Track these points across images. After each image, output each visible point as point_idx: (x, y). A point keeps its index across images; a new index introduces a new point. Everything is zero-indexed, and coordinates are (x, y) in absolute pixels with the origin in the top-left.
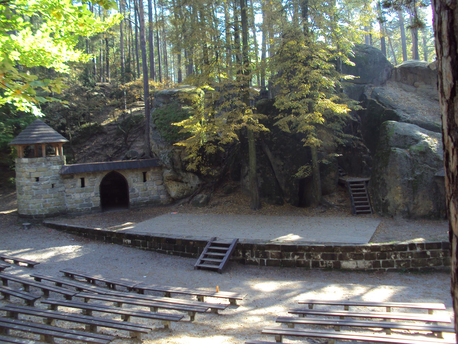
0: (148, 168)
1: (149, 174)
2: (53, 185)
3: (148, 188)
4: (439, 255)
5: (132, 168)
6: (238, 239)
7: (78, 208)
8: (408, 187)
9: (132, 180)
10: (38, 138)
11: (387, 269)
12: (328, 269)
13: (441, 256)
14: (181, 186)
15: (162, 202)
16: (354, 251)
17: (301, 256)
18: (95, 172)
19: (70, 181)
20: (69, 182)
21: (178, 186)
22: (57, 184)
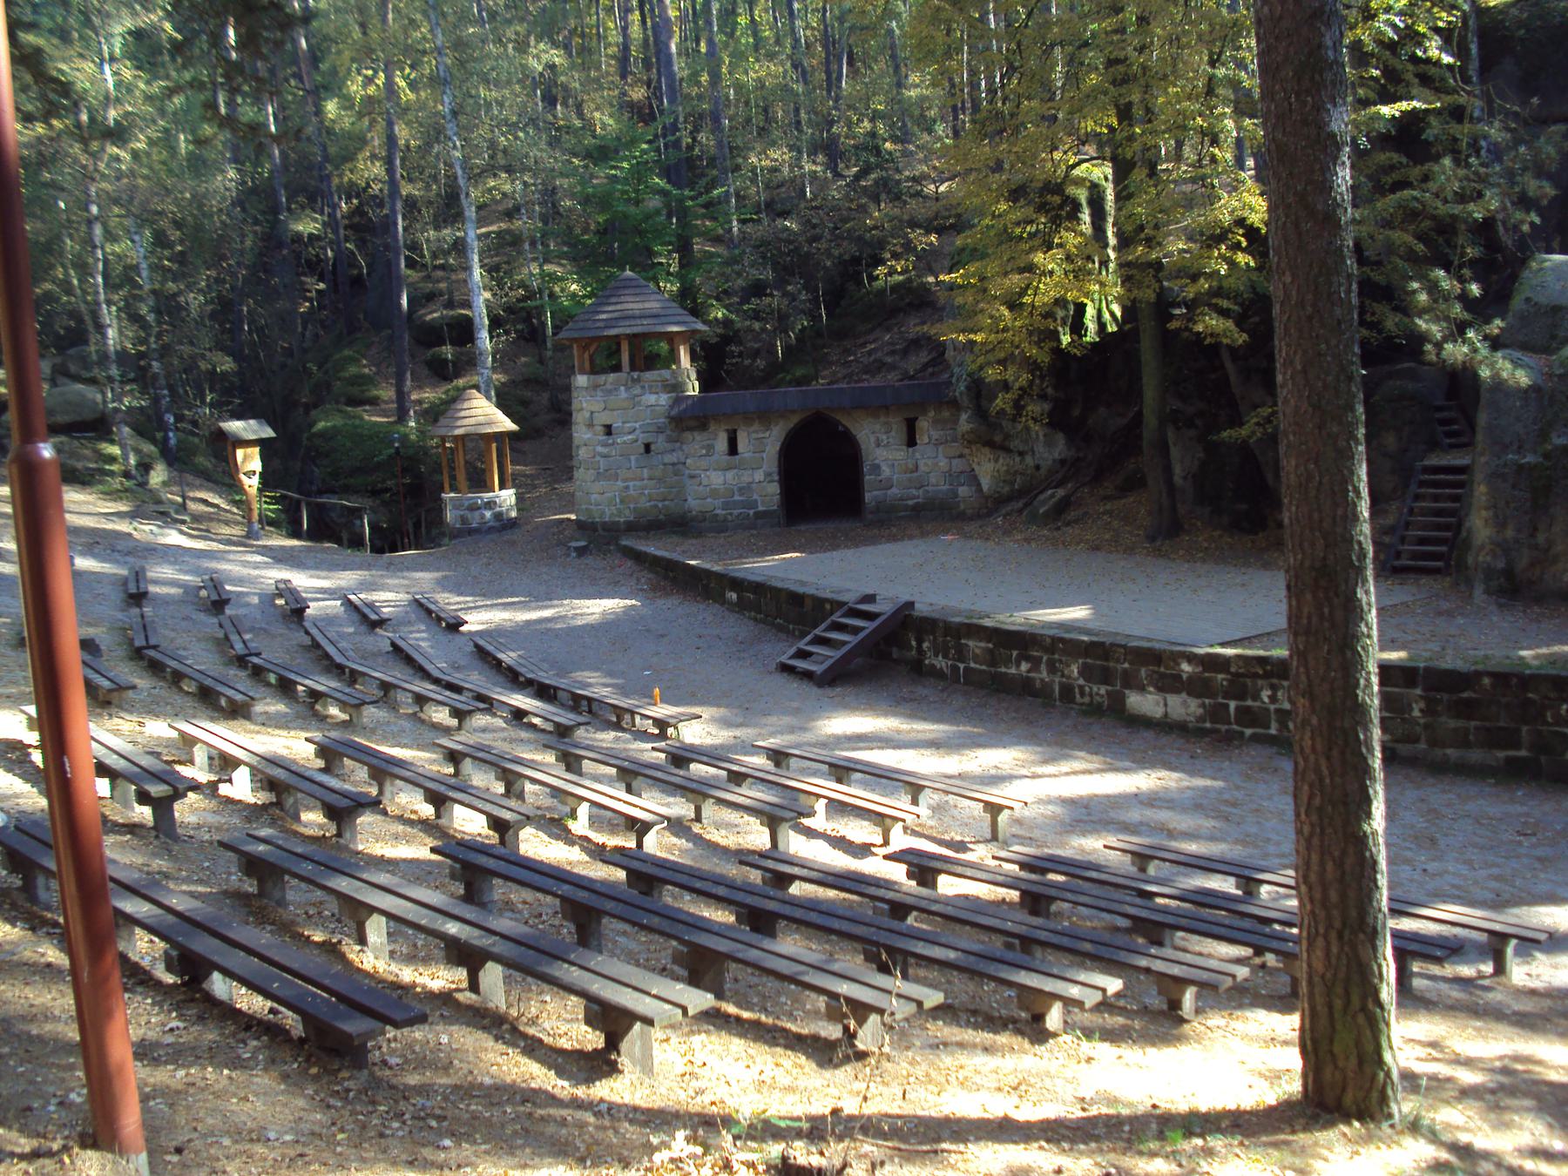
0: (922, 407)
1: (923, 424)
2: (647, 448)
3: (921, 463)
4: (1412, 709)
5: (875, 405)
6: (912, 604)
7: (718, 511)
8: (1514, 487)
9: (873, 439)
10: (609, 324)
11: (1248, 732)
12: (1094, 711)
13: (1416, 713)
14: (1004, 463)
15: (962, 507)
16: (1156, 665)
17: (1036, 664)
18: (764, 416)
19: (698, 436)
20: (695, 443)
21: (996, 461)
22: (660, 443)
